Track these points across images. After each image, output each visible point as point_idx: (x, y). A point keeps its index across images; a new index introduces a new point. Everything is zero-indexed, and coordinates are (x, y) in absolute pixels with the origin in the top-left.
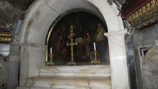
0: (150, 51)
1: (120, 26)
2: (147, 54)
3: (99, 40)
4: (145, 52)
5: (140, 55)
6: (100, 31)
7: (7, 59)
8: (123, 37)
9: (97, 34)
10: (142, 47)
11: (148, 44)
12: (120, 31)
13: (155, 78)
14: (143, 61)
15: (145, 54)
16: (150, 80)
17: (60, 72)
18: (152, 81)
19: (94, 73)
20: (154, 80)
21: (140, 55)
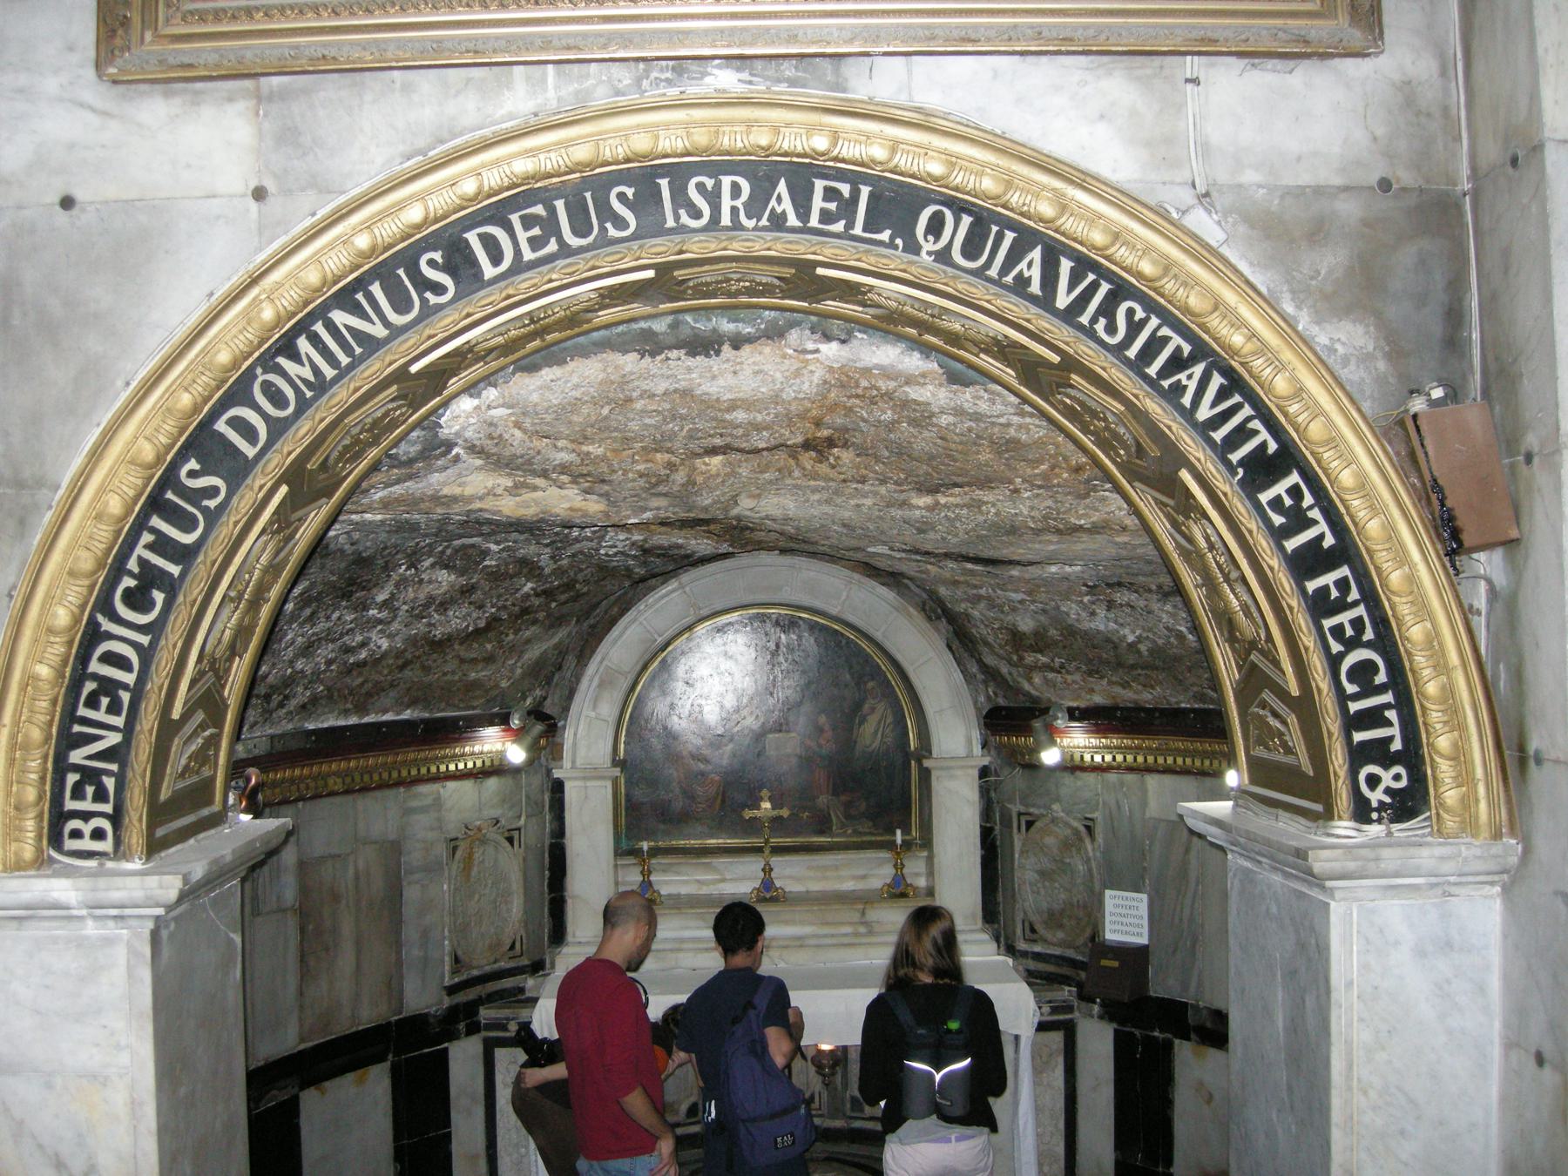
0: (1038, 824)
1: (969, 741)
2: (1032, 830)
3: (870, 749)
4: (1030, 824)
5: (1015, 830)
6: (873, 710)
7: (516, 834)
8: (976, 773)
9: (861, 724)
10: (1022, 809)
11: (1039, 807)
12: (970, 755)
13: (1044, 887)
14: (1024, 845)
15: (1028, 829)
16: (1033, 892)
17: (723, 880)
18: (1038, 893)
19: (864, 877)
20: (1042, 892)
21: (1015, 830)
